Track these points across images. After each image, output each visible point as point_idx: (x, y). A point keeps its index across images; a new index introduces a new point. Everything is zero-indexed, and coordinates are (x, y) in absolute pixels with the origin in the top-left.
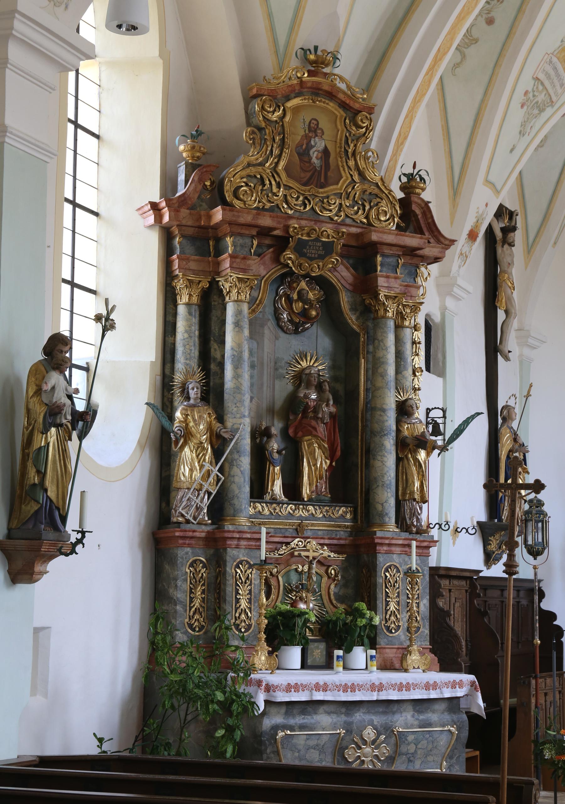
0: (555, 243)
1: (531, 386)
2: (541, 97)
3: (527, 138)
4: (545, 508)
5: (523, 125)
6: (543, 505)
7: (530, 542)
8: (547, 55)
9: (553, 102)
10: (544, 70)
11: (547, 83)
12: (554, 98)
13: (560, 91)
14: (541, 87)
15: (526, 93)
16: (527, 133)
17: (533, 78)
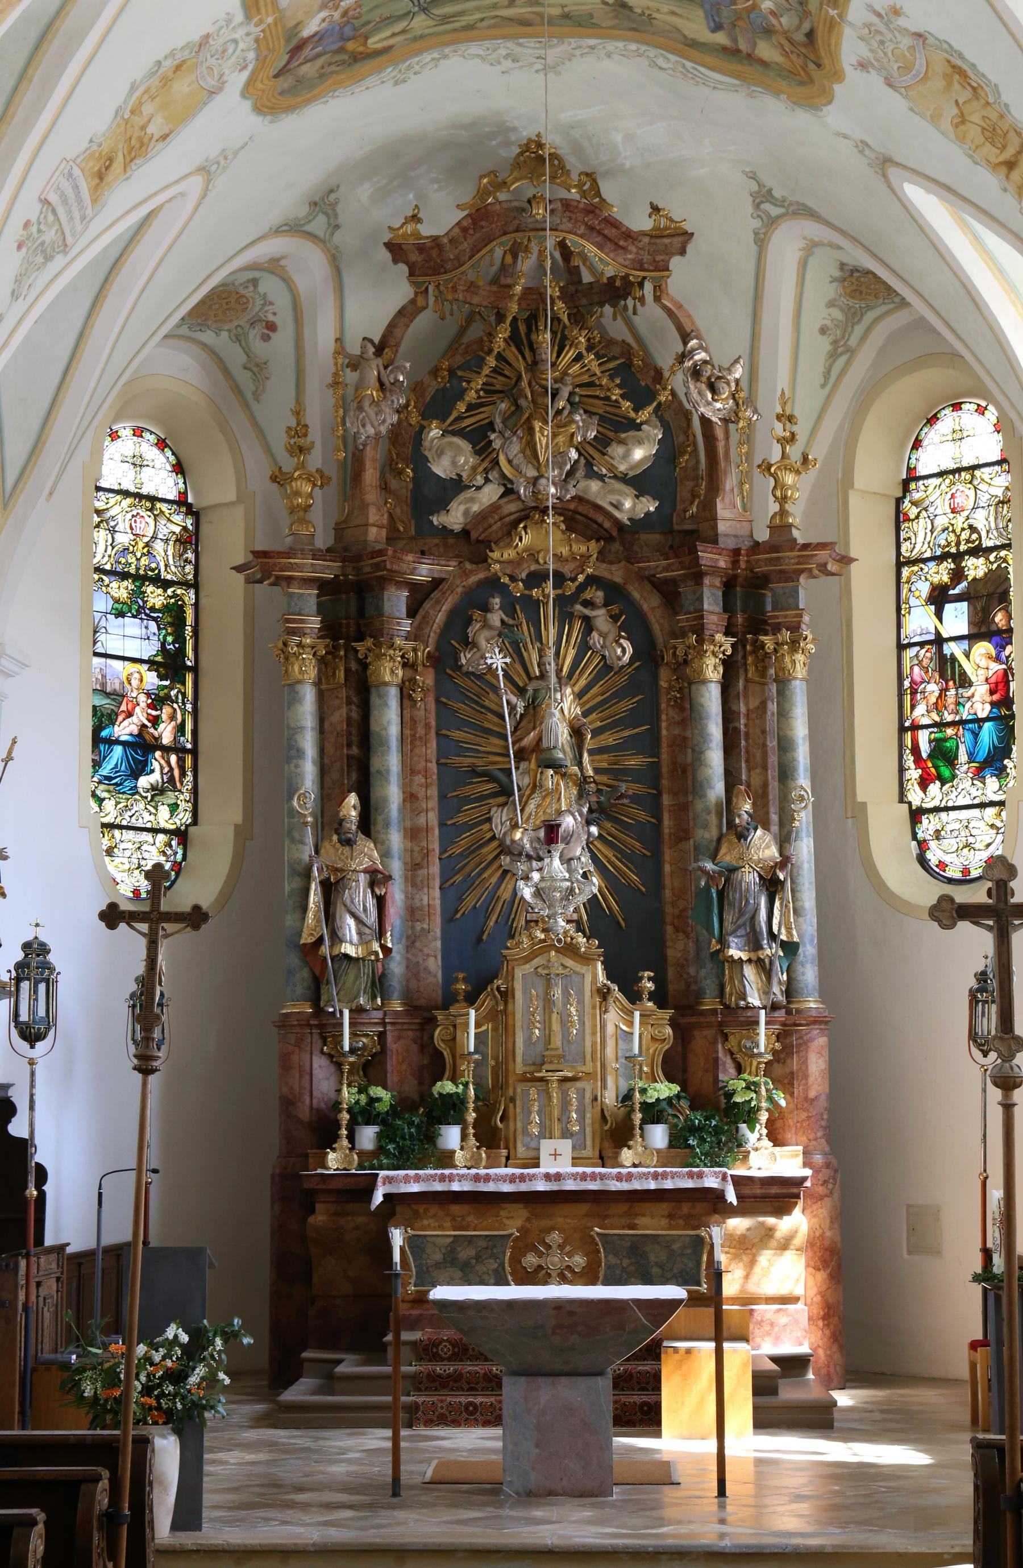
0: (51, 494)
1: (14, 742)
2: (50, 235)
3: (21, 305)
4: (51, 957)
5: (18, 280)
6: (48, 952)
7: (24, 1017)
8: (65, 162)
9: (66, 245)
10: (59, 188)
11: (61, 211)
12: (69, 240)
13: (79, 228)
14: (51, 218)
15: (27, 224)
16: (22, 297)
17: (40, 200)
